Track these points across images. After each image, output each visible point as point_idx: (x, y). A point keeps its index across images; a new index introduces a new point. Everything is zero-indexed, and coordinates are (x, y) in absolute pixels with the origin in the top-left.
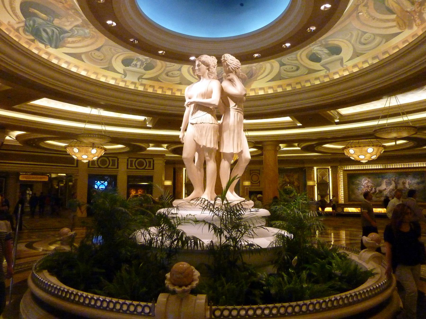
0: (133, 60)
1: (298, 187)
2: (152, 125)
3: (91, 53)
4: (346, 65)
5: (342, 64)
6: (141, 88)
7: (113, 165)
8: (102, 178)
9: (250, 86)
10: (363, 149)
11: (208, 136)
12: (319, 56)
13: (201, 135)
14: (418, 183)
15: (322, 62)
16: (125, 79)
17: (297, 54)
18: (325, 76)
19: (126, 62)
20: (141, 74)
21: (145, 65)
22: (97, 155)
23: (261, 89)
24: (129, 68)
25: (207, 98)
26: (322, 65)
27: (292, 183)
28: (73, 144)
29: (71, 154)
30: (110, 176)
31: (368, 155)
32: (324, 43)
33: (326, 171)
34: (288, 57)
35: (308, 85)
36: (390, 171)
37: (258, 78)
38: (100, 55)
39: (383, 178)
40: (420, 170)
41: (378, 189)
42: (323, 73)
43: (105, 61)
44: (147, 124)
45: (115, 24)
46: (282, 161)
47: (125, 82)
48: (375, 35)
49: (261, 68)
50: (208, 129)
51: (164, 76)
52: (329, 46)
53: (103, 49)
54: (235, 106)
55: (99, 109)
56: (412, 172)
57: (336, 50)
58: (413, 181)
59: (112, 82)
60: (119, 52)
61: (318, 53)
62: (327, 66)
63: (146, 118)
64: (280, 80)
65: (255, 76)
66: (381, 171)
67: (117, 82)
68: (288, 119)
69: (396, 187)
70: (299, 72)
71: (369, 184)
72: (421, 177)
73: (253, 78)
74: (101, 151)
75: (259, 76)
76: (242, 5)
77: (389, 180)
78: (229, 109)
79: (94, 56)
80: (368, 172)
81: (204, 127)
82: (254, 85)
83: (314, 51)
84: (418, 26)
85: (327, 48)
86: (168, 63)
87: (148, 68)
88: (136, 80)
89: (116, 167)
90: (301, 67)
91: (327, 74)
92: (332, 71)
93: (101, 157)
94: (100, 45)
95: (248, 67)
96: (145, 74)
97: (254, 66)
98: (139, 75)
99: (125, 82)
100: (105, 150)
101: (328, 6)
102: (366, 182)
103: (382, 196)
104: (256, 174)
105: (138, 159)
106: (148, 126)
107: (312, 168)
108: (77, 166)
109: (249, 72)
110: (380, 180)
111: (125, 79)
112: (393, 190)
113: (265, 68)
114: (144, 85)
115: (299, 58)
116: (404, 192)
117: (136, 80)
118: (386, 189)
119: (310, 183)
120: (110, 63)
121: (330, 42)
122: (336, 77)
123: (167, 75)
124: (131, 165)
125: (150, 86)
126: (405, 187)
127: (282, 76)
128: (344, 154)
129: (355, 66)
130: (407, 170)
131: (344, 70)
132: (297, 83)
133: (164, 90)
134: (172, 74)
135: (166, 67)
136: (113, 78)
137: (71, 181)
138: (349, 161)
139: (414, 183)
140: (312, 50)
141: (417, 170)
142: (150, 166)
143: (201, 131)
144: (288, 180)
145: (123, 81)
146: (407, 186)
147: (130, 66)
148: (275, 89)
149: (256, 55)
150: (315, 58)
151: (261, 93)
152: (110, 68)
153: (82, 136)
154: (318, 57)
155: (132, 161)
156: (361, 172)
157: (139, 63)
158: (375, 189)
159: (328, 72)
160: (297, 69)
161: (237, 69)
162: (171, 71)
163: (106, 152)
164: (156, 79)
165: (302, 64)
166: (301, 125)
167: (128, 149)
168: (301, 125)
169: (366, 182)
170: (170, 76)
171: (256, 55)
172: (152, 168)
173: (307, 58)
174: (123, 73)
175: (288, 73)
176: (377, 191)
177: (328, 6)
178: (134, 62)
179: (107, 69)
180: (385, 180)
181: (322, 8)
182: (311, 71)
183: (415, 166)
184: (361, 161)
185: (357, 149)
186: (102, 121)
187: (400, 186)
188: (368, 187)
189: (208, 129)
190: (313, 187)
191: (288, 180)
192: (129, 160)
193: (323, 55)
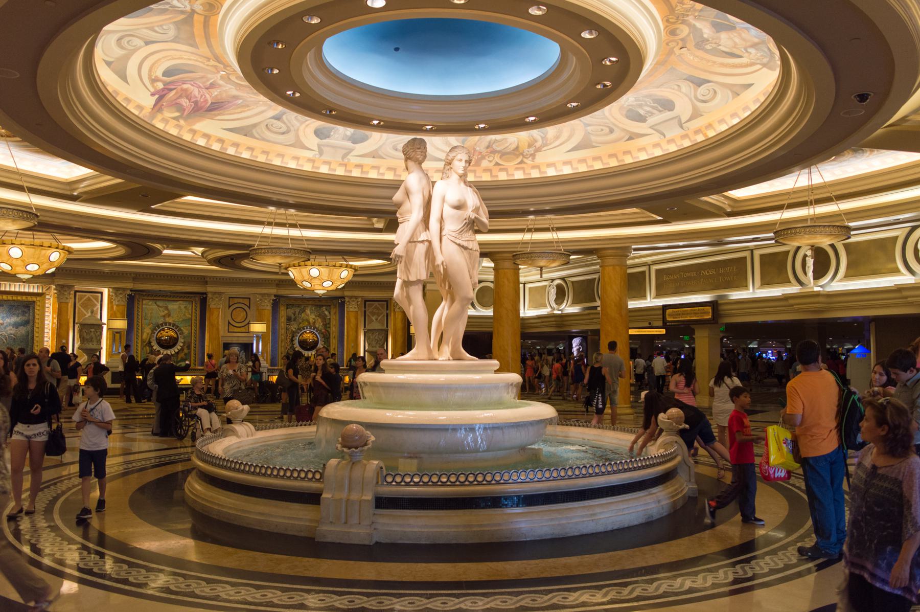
4: (349, 160)
5: (345, 156)
10: (44, 252)
14: (16, 325)
26: (319, 146)
31: (44, 267)
42: (309, 154)
56: (8, 300)
57: (363, 139)
58: (8, 320)
72: (24, 313)
76: (397, 49)
82: (205, 125)
92: (324, 158)
122: (324, 169)
129: (360, 166)
131: (341, 165)
132: (264, 152)
139: (10, 324)
141: (19, 298)
148: (224, 146)
151: (201, 142)
160: (283, 133)
165: (298, 130)
183: (13, 289)
184: (18, 276)
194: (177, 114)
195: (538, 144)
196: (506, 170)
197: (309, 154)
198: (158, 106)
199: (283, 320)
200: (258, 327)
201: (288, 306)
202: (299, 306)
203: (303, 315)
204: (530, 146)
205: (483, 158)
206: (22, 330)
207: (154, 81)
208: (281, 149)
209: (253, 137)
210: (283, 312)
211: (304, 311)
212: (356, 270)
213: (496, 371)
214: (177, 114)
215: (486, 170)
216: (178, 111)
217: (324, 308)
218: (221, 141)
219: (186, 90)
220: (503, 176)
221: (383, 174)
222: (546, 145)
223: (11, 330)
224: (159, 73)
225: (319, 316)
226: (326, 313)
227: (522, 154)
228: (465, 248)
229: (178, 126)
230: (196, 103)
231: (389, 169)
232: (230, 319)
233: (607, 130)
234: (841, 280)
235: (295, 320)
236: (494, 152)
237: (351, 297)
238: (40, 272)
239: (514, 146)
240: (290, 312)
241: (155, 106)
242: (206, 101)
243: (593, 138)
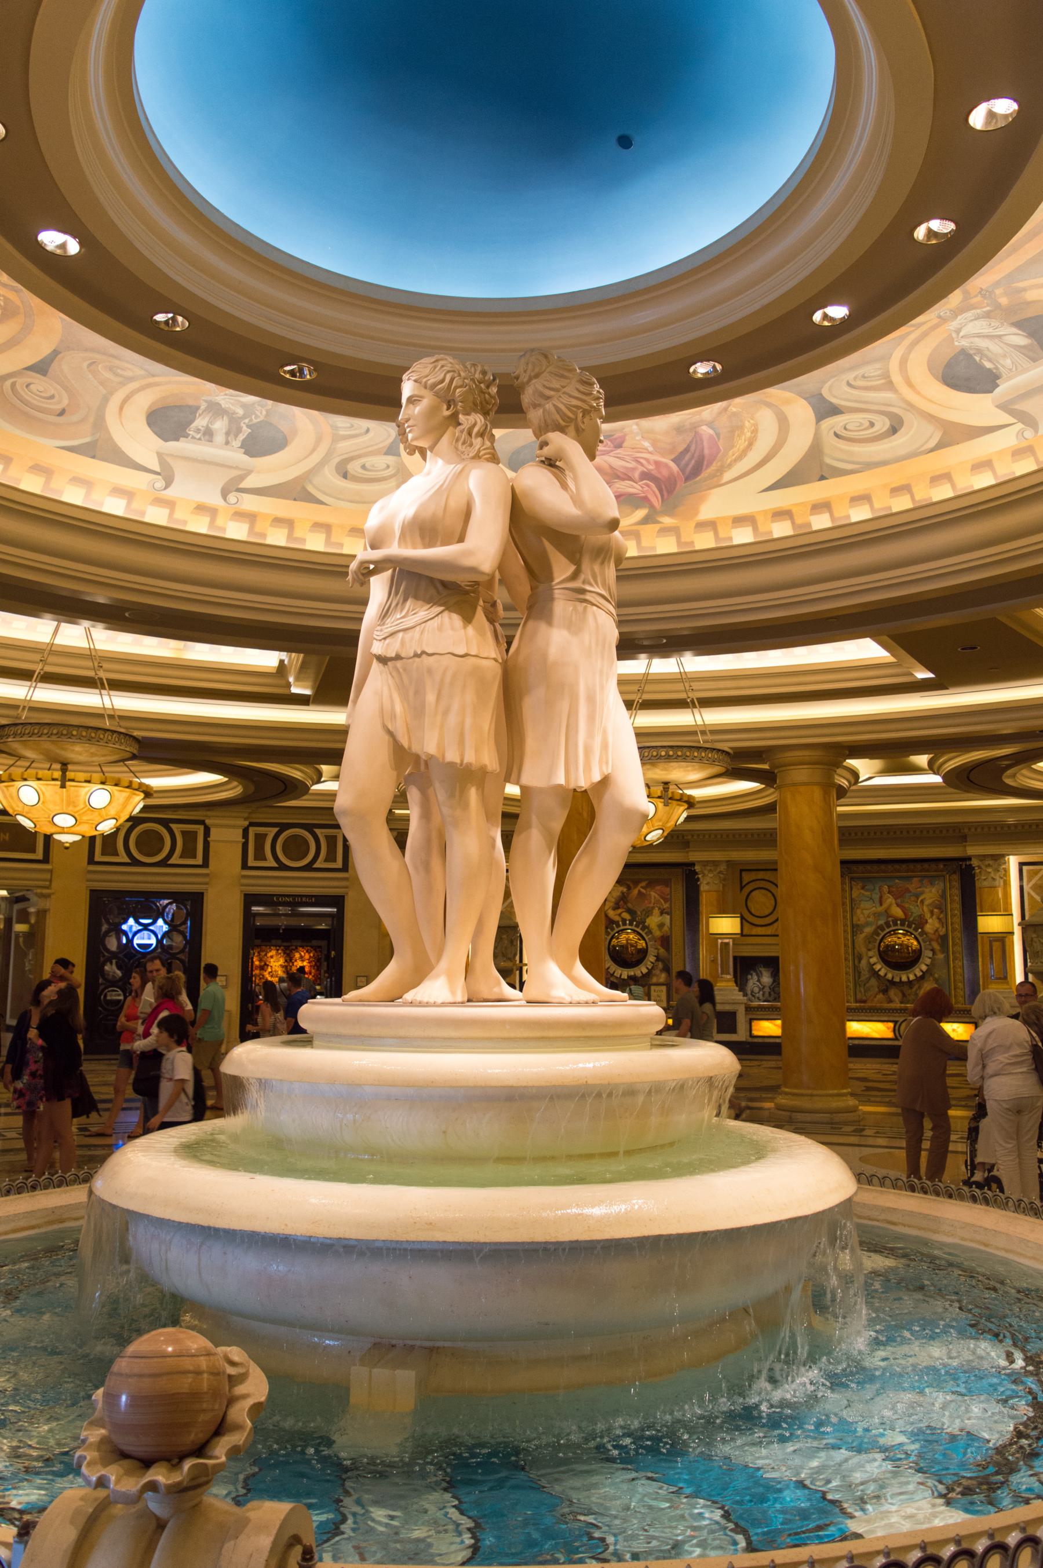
0: (192, 411)
1: (943, 940)
2: (313, 688)
3: (13, 385)
6: (236, 531)
7: (189, 851)
8: (144, 905)
9: (696, 512)
11: (446, 712)
12: (988, 365)
13: (417, 710)
15: (1004, 388)
16: (171, 493)
17: (886, 358)
18: (1018, 453)
19: (169, 421)
20: (235, 473)
21: (246, 431)
22: (112, 812)
23: (739, 521)
25: (444, 544)
26: (1004, 407)
27: (914, 925)
28: (16, 771)
29: (10, 811)
30: (177, 897)
32: (1004, 301)
34: (850, 376)
35: (943, 492)
37: (727, 476)
38: (53, 392)
42: (1008, 439)
43: (75, 418)
44: (289, 685)
45: (73, 247)
46: (852, 833)
47: (170, 504)
49: (736, 429)
50: (448, 680)
51: (329, 476)
52: (1030, 313)
53: (64, 366)
54: (575, 576)
55: (86, 623)
59: (115, 507)
60: (131, 379)
61: (979, 351)
62: (1028, 406)
63: (284, 655)
64: (822, 478)
65: (713, 468)
67: (135, 505)
68: (865, 650)
70: (899, 443)
73: (705, 474)
74: (128, 799)
75: (730, 466)
76: (625, 142)
78: (551, 589)
79: (27, 397)
81: (430, 671)
82: (715, 504)
83: (965, 343)
85: (1019, 325)
86: (342, 422)
87: (261, 443)
88: (215, 499)
89: (199, 861)
90: (907, 417)
91: (1024, 444)
93: (134, 821)
94: (46, 351)
95: (679, 429)
96: (249, 472)
97: (706, 417)
98: (224, 477)
99: (170, 504)
100: (148, 793)
101: (1005, 107)
105: (283, 827)
106: (295, 690)
107: (999, 859)
108: (46, 859)
109: (687, 450)
111: (171, 493)
113: (755, 431)
114: (251, 518)
115: (897, 378)
117: (215, 499)
119: (989, 924)
120: (100, 424)
121: (1031, 295)
123: (345, 476)
124: (260, 855)
125: (278, 521)
127: (828, 460)
132: (896, 491)
133: (334, 539)
134: (363, 467)
135: (337, 439)
136: (118, 491)
137: (24, 917)
140: (950, 339)
142: (331, 857)
143: (416, 693)
144: (898, 912)
145: (159, 502)
147: (186, 436)
148: (798, 521)
149: (701, 369)
150: (967, 375)
151: (743, 536)
152: (101, 448)
153: (15, 735)
154: (980, 367)
155: (260, 839)
157: (220, 425)
159: (1029, 434)
160: (894, 430)
161: (585, 413)
162: (359, 456)
163: (151, 802)
164: (297, 491)
166: (931, 675)
167: (235, 790)
168: (931, 675)
170: (357, 479)
171: (701, 369)
172: (339, 864)
173: (937, 378)
174: (158, 469)
175: (856, 448)
177: (1005, 107)
178: (201, 422)
179: (89, 450)
181: (977, 119)
182: (953, 434)
186: (102, 675)
189: (448, 680)
190: (1002, 939)
191: (898, 912)
192: (252, 831)
193: (1005, 356)
197: (1008, 439)
216: (637, 507)
218: (780, 514)
229: (665, 531)
230: (646, 476)
242: (657, 464)
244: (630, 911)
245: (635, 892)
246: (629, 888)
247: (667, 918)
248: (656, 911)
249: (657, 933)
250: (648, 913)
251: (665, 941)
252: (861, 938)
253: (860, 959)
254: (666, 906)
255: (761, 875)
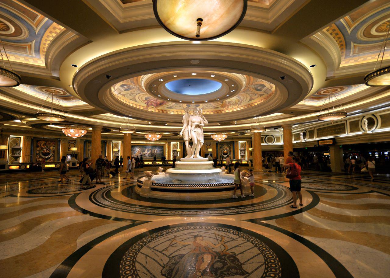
14: (160, 151)
24: (121, 88)
33: (118, 143)
36: (149, 145)
39: (146, 148)
40: (161, 145)
41: (143, 153)
48: (213, 106)
66: (146, 145)
69: (151, 152)
71: (139, 151)
76: (190, 85)
77: (149, 149)
80: (139, 145)
84: (226, 108)
102: (138, 149)
103: (145, 157)
104: (74, 143)
110: (144, 149)
112: (150, 154)
116: (154, 154)
118: (147, 153)
126: (155, 153)
128: (144, 136)
130: (156, 145)
138: (145, 139)
146: (156, 152)
156: (136, 145)
158: (142, 153)
160: (180, 107)
164: (124, 95)
169: (138, 149)
171: (181, 102)
176: (143, 154)
180: (147, 149)
185: (153, 135)
187: (153, 152)
188: (139, 152)
194: (153, 107)
195: (240, 101)
196: (235, 108)
198: (148, 106)
199: (219, 148)
200: (210, 150)
201: (220, 144)
202: (222, 144)
203: (224, 146)
204: (239, 101)
205: (229, 106)
206: (161, 152)
207: (144, 101)
208: (180, 110)
209: (173, 109)
210: (219, 146)
211: (224, 145)
212: (228, 135)
213: (208, 161)
214: (153, 107)
215: (230, 109)
217: (229, 145)
219: (152, 102)
220: (235, 110)
221: (206, 113)
222: (242, 101)
223: (159, 152)
224: (144, 99)
225: (228, 146)
226: (230, 146)
227: (238, 104)
228: (196, 132)
231: (207, 112)
232: (206, 148)
233: (254, 95)
234: (379, 128)
235: (222, 148)
236: (231, 104)
237: (235, 141)
238: (156, 140)
239: (235, 102)
240: (221, 146)
241: (147, 106)
243: (252, 97)
244: (47, 146)
245: (48, 143)
246: (46, 142)
247: (54, 148)
248: (52, 146)
249: (52, 150)
250: (51, 146)
251: (54, 152)
252: (89, 151)
253: (89, 154)
254: (54, 145)
255: (72, 141)
